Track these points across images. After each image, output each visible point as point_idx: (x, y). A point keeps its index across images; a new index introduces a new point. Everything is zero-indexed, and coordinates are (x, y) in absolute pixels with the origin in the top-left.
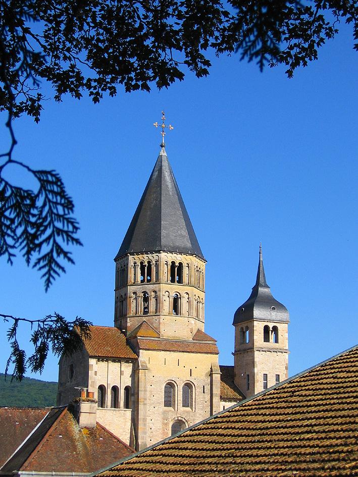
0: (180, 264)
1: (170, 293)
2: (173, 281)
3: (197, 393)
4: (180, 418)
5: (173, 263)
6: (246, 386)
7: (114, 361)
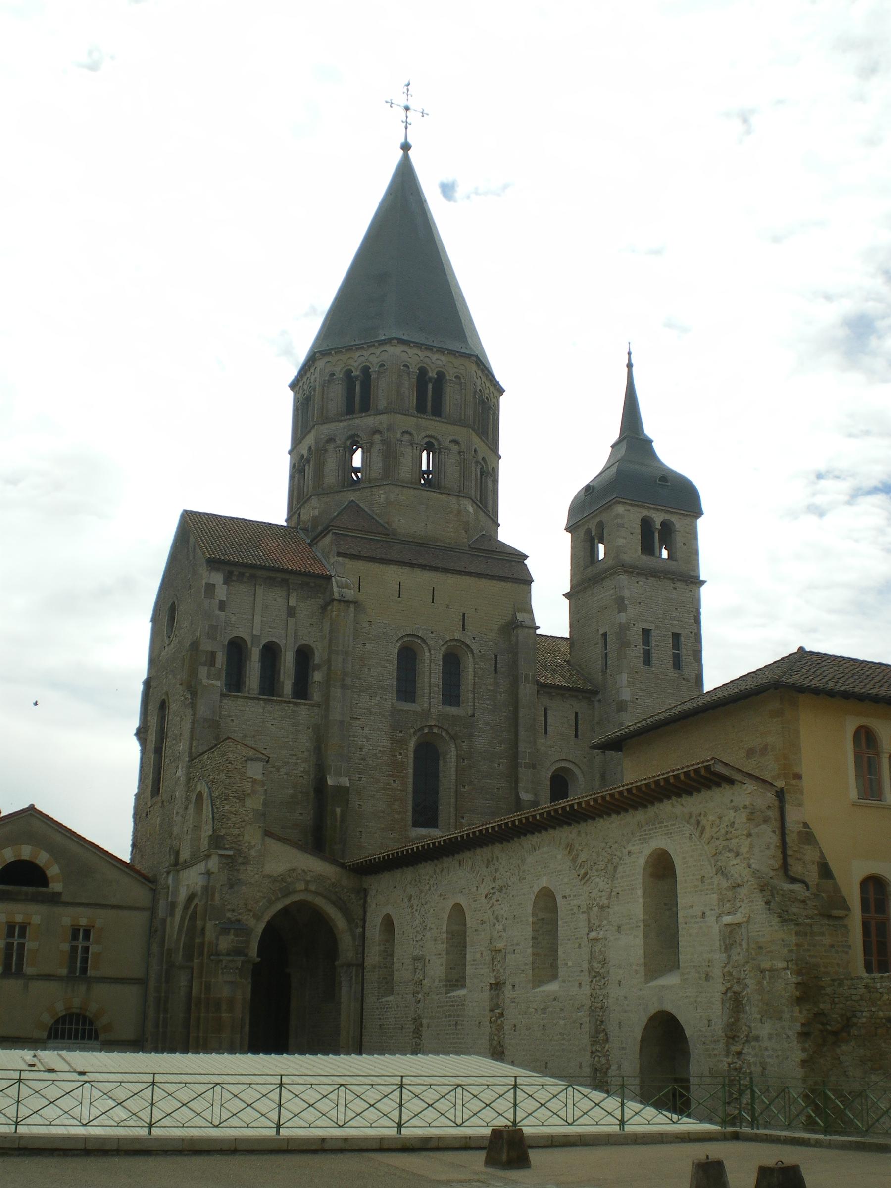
0: (441, 376)
2: (421, 408)
4: (435, 730)
5: (423, 372)
7: (271, 582)
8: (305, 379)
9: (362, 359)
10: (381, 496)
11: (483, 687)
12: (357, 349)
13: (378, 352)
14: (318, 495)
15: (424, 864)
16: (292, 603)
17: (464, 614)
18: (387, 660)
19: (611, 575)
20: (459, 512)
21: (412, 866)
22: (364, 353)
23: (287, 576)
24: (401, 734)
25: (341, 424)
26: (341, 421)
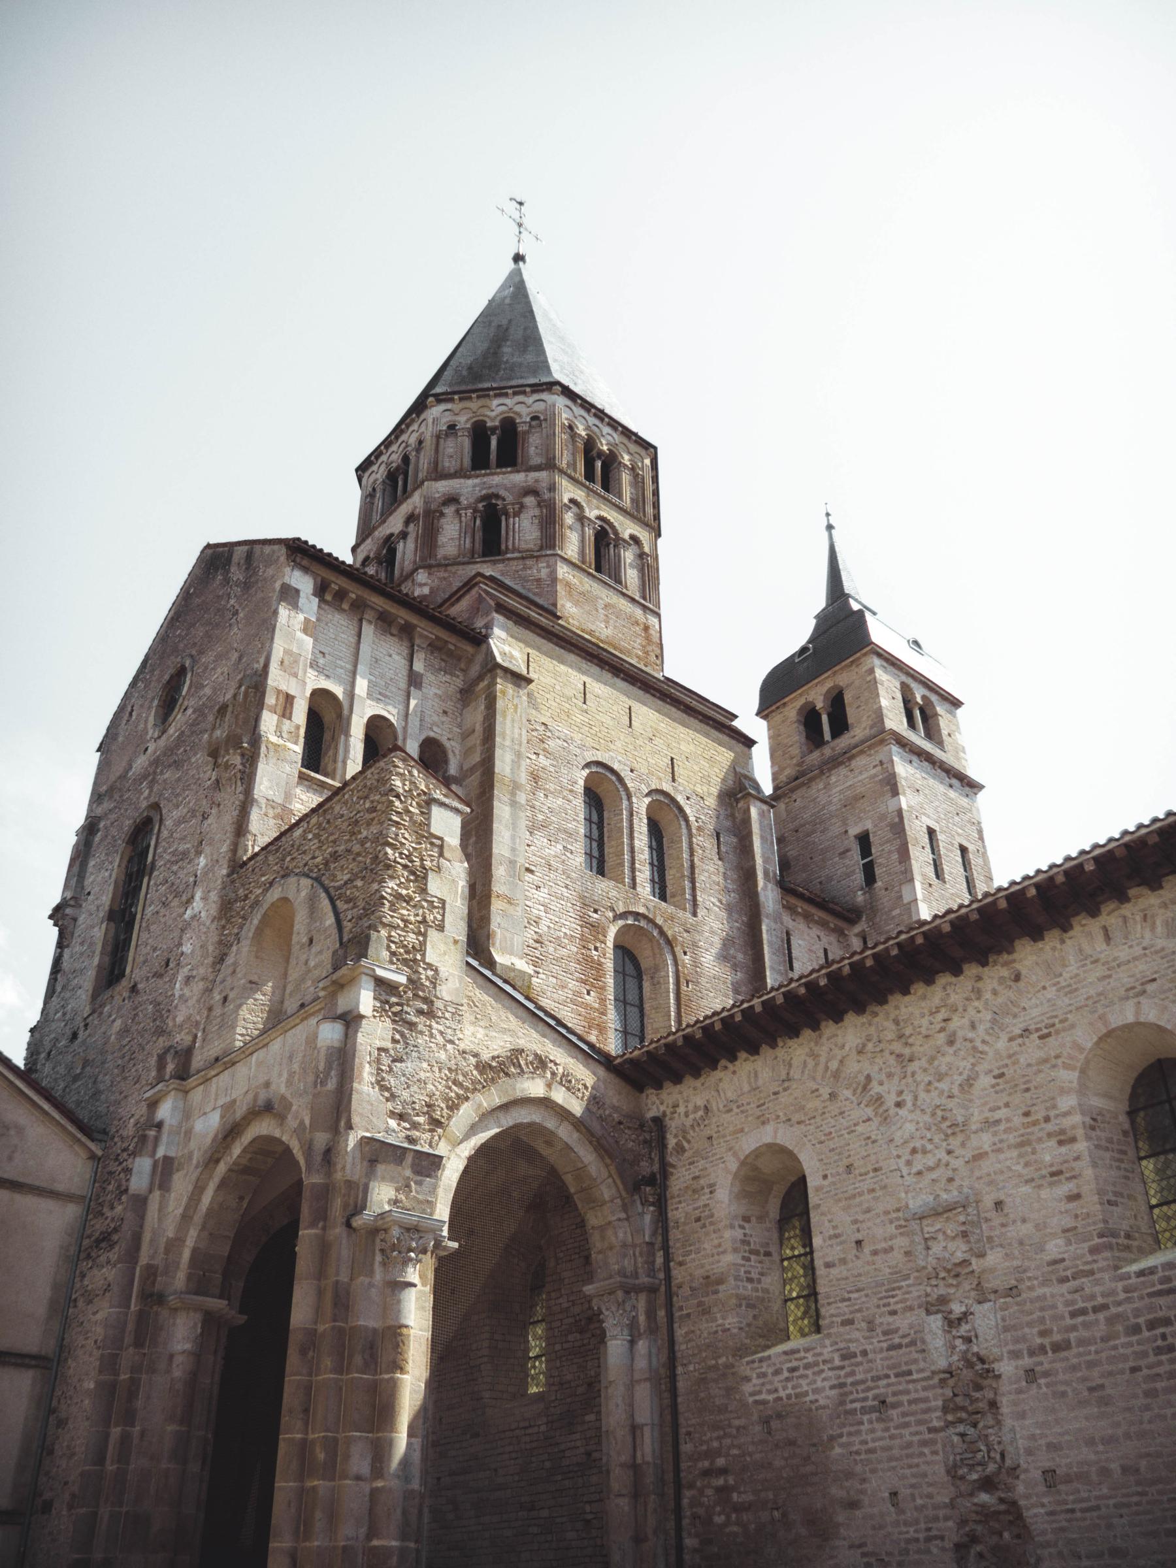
1: (587, 510)
3: (699, 852)
6: (859, 877)
8: (394, 448)
9: (503, 408)
10: (541, 570)
11: (706, 874)
12: (496, 396)
13: (530, 400)
14: (429, 567)
15: (919, 988)
16: (418, 666)
17: (672, 759)
18: (571, 791)
19: (870, 748)
20: (646, 628)
21: (860, 1009)
22: (507, 401)
23: (413, 619)
24: (595, 916)
25: (470, 482)
26: (469, 478)
